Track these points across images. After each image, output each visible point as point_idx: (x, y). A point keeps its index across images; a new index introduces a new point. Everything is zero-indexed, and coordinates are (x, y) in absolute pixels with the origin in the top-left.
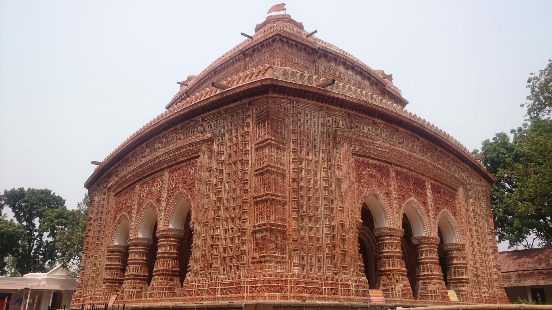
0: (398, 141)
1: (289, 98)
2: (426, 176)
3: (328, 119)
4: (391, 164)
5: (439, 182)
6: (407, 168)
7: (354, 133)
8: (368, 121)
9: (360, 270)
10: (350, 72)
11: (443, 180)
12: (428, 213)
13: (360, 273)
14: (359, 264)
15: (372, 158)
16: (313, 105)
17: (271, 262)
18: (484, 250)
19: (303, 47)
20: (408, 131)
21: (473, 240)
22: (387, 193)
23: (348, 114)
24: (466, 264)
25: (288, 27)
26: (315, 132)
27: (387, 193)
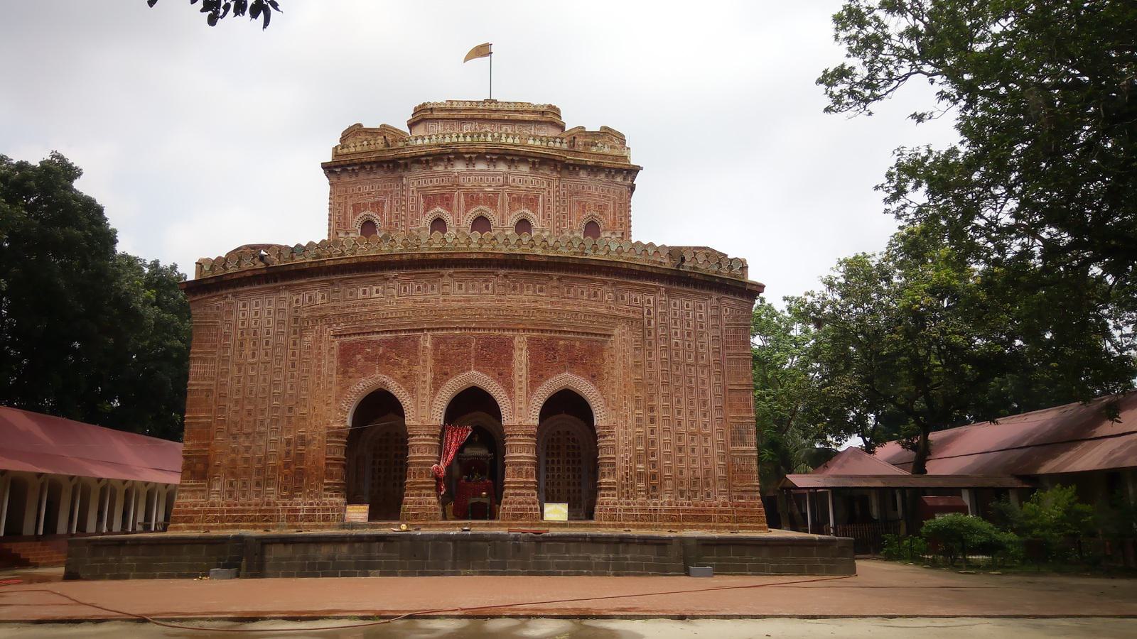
0: (441, 291)
1: (219, 293)
2: (513, 330)
3: (295, 298)
4: (422, 330)
5: (551, 331)
6: (460, 329)
7: (334, 308)
8: (371, 279)
9: (325, 490)
10: (481, 166)
11: (563, 326)
12: (509, 388)
13: (327, 493)
14: (326, 481)
15: (378, 332)
16: (263, 289)
17: (183, 491)
18: (693, 429)
19: (374, 166)
20: (466, 270)
21: (655, 414)
22: (405, 377)
23: (327, 281)
24: (614, 458)
25: (352, 145)
26: (269, 323)
27: (405, 378)
